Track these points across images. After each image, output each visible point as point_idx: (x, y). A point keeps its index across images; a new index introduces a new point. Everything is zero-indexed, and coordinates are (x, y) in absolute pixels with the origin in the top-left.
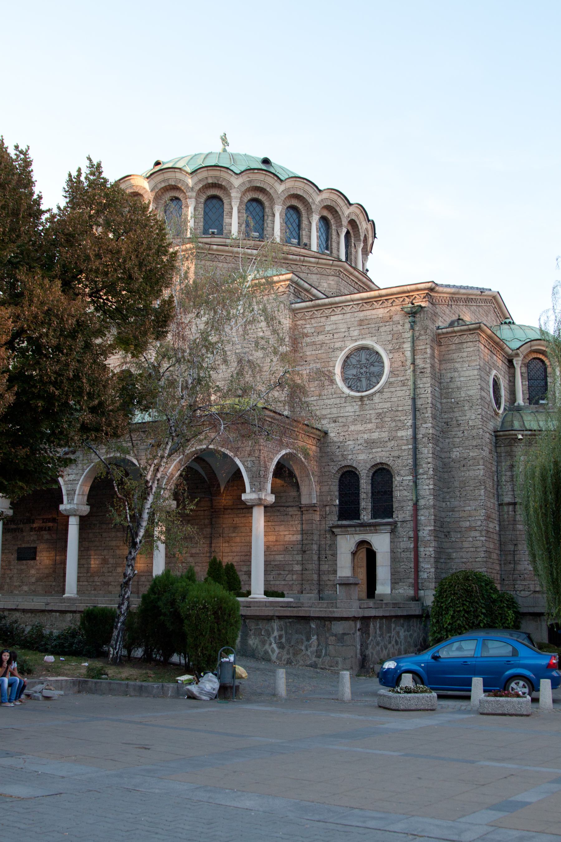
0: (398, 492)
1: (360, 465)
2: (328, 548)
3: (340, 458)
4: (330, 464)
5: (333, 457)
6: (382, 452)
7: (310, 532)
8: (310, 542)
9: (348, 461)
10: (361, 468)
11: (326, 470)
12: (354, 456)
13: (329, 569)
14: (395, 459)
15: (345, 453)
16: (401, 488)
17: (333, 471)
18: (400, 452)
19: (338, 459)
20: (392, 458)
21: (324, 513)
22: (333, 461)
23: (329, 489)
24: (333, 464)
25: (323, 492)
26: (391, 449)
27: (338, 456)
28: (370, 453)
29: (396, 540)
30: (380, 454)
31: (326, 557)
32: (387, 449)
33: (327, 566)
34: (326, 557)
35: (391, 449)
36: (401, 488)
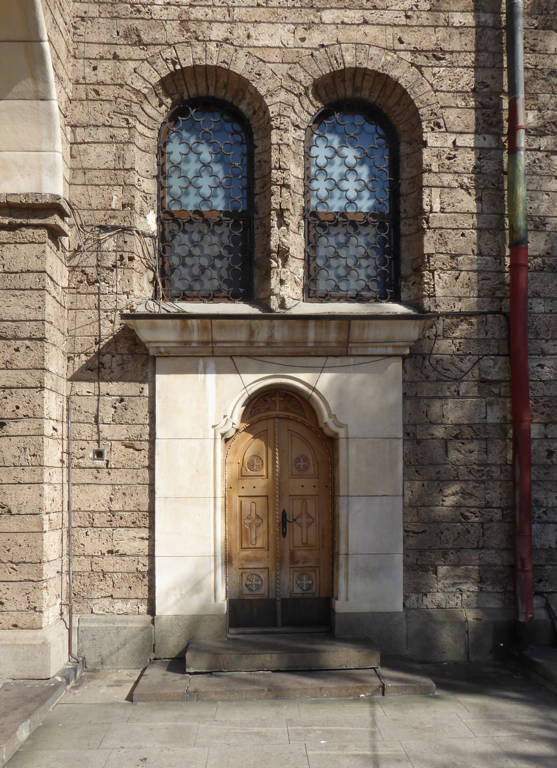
0: (436, 192)
1: (267, 69)
2: (107, 413)
3: (173, 29)
4: (122, 52)
5: (137, 24)
6: (368, 29)
7: (26, 329)
8: (31, 381)
9: (212, 47)
10: (272, 85)
11: (101, 76)
12: (240, 31)
13: (116, 506)
14: (421, 60)
15: (198, 13)
16: (447, 179)
17: (139, 85)
18: (442, 33)
19: (160, 36)
20: (408, 57)
21: (92, 260)
22: (140, 43)
23: (120, 158)
24: (137, 52)
25: (85, 171)
26: (403, 21)
27: (162, 23)
28: (309, 26)
29: (426, 389)
30: (356, 34)
31: (99, 454)
32: (388, 17)
33: (104, 492)
34: (99, 454)
35: (403, 21)
36: (447, 179)
